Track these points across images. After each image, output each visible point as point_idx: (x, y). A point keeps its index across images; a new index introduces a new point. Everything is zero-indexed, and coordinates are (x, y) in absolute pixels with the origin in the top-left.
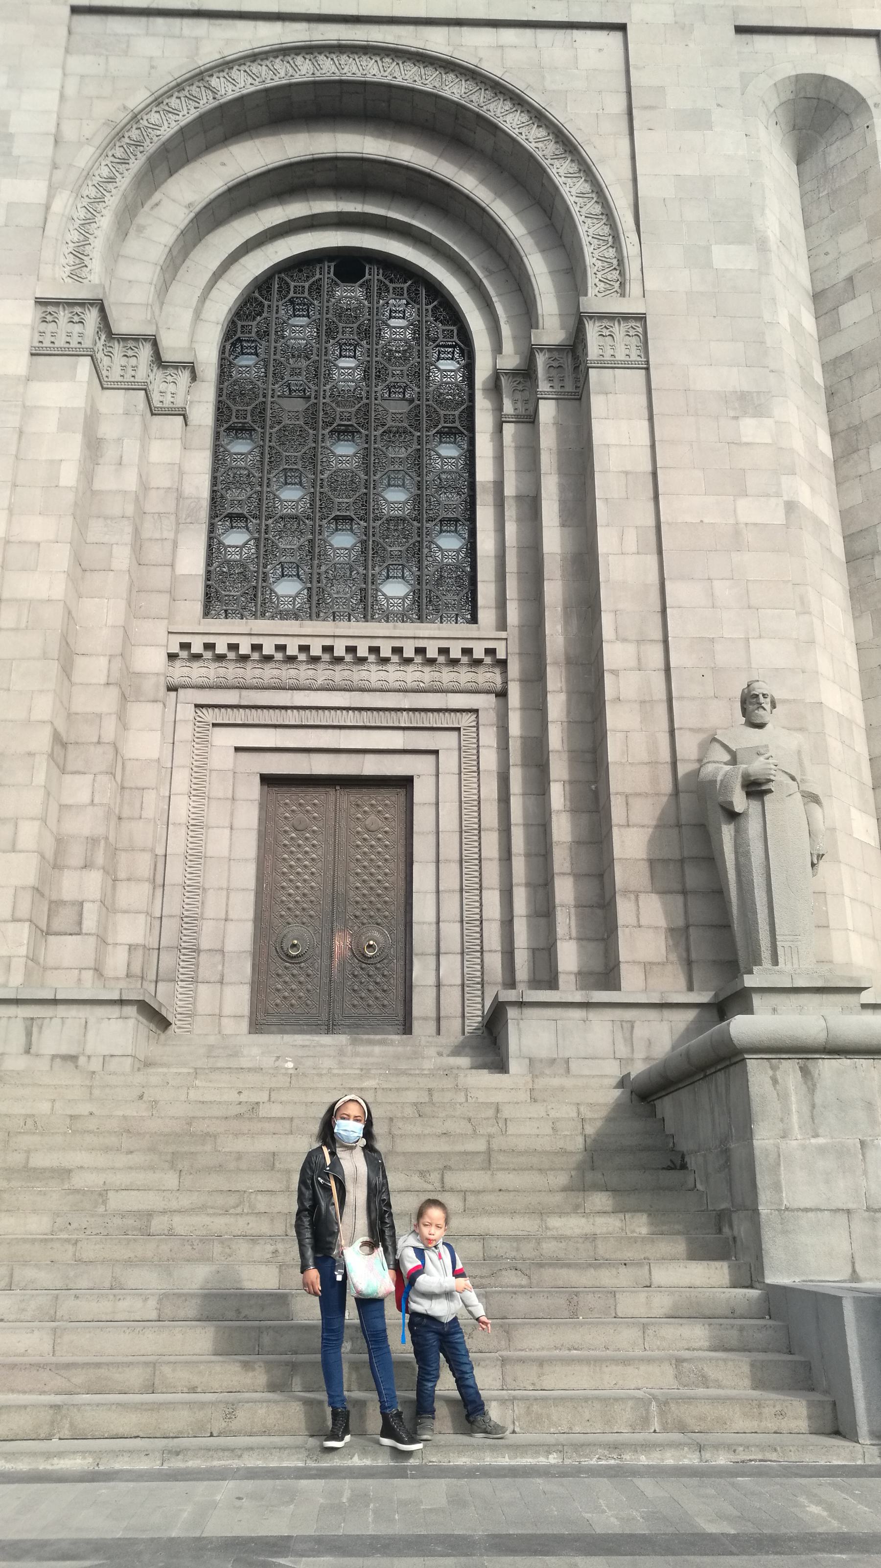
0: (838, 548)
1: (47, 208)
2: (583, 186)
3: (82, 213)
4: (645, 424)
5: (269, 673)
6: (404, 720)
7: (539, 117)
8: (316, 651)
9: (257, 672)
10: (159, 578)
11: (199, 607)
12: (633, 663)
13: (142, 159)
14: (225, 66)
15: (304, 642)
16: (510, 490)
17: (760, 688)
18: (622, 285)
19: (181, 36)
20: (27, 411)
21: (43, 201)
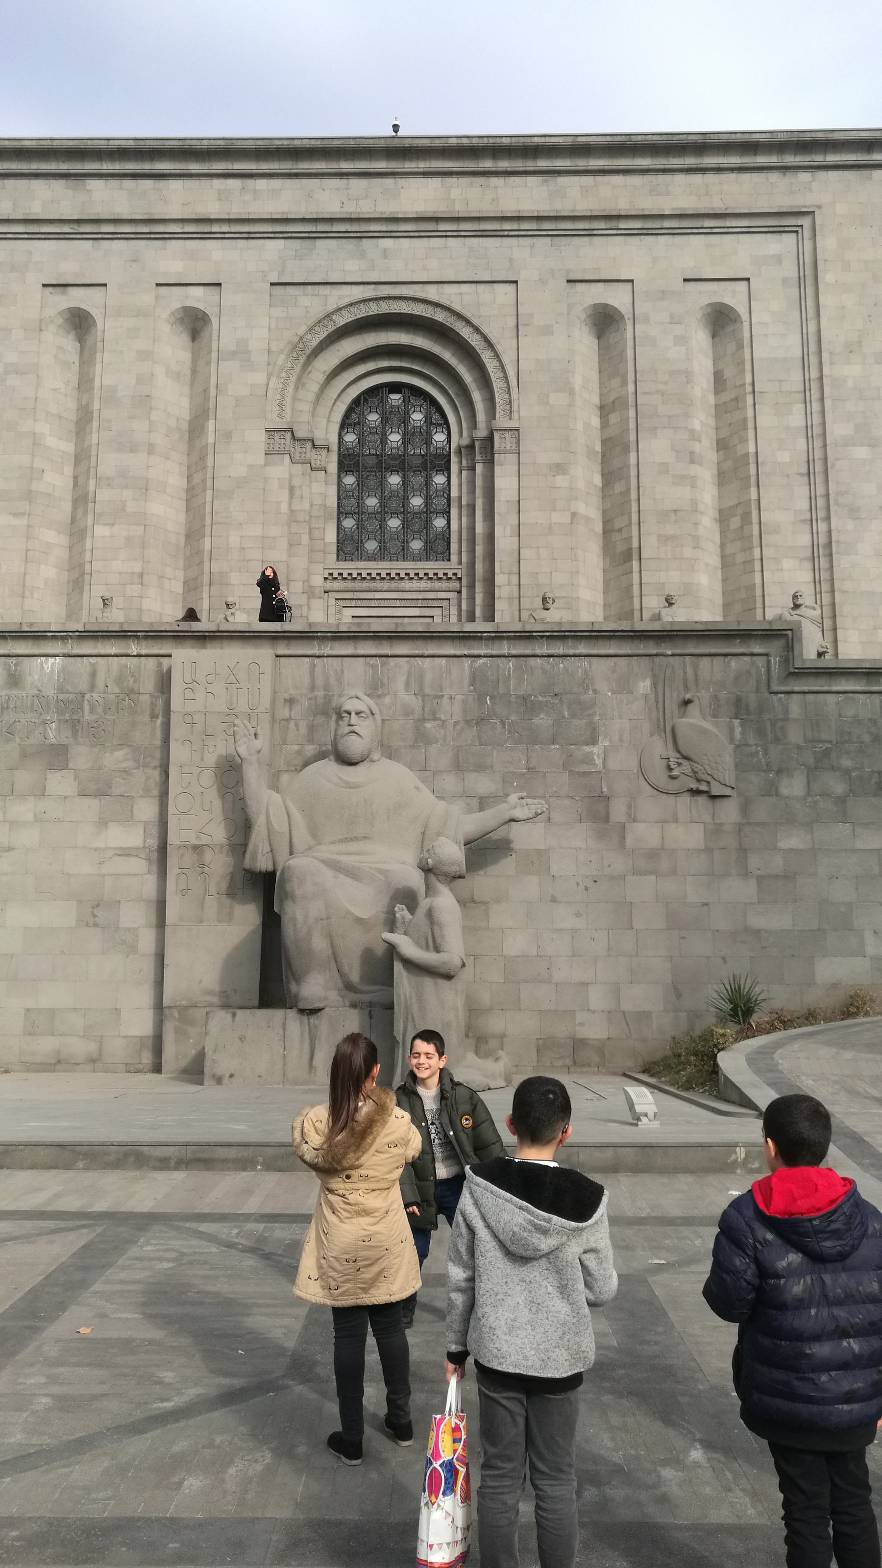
0: (599, 527)
1: (268, 384)
2: (495, 363)
3: (281, 385)
4: (517, 478)
5: (365, 585)
6: (420, 603)
7: (477, 330)
8: (383, 575)
9: (360, 585)
10: (319, 545)
11: (335, 556)
12: (507, 583)
13: (305, 357)
15: (379, 571)
16: (464, 502)
17: (548, 595)
18: (511, 412)
19: (318, 295)
20: (266, 480)
21: (265, 383)
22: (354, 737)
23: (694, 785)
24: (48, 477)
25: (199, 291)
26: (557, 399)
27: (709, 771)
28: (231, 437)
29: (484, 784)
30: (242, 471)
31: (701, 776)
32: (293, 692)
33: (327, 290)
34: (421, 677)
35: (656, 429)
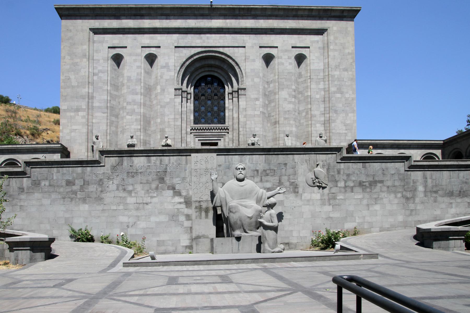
7: (234, 60)
13: (185, 68)
14: (195, 55)
20: (175, 102)
22: (241, 174)
23: (319, 184)
24: (112, 102)
25: (154, 49)
26: (256, 80)
27: (322, 181)
28: (164, 91)
29: (268, 185)
30: (168, 100)
31: (321, 182)
32: (220, 163)
33: (191, 49)
34: (252, 159)
35: (283, 88)
